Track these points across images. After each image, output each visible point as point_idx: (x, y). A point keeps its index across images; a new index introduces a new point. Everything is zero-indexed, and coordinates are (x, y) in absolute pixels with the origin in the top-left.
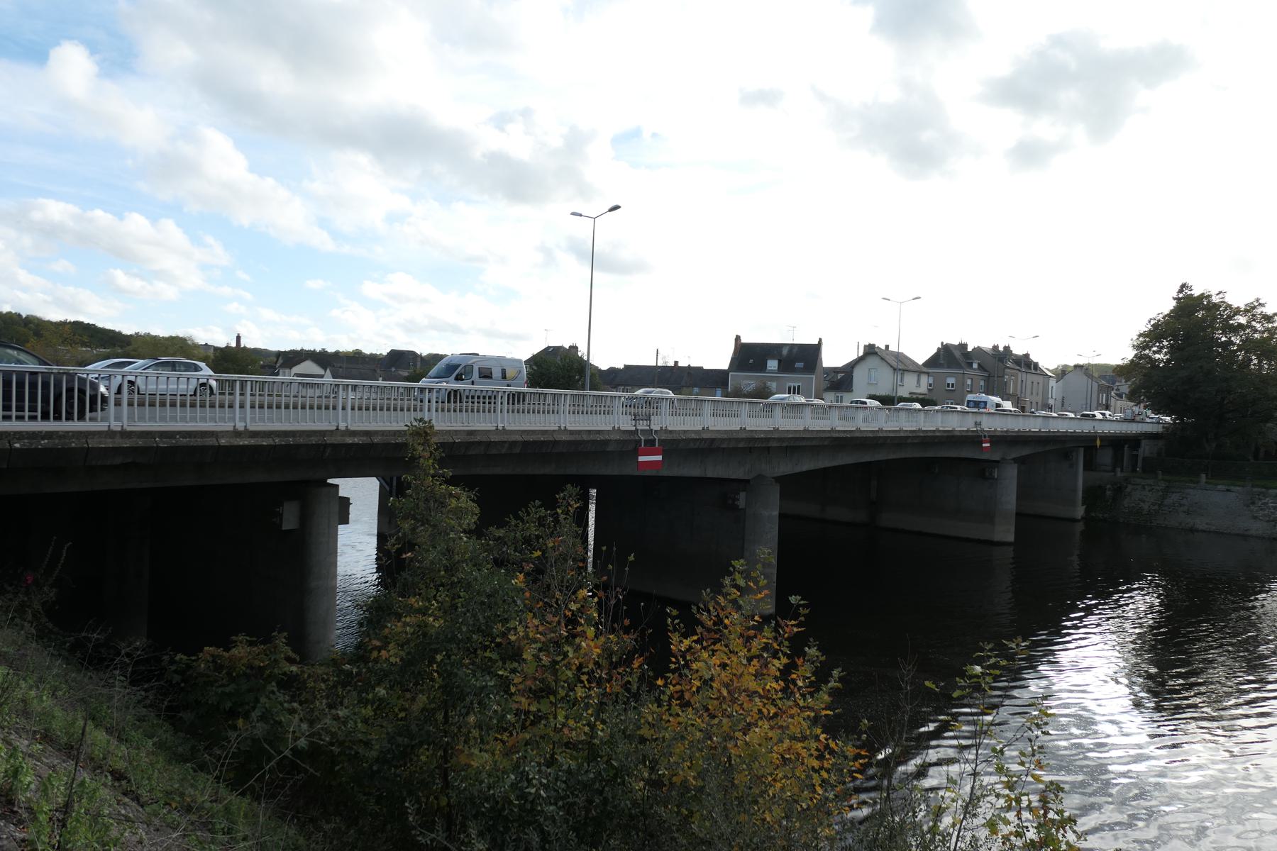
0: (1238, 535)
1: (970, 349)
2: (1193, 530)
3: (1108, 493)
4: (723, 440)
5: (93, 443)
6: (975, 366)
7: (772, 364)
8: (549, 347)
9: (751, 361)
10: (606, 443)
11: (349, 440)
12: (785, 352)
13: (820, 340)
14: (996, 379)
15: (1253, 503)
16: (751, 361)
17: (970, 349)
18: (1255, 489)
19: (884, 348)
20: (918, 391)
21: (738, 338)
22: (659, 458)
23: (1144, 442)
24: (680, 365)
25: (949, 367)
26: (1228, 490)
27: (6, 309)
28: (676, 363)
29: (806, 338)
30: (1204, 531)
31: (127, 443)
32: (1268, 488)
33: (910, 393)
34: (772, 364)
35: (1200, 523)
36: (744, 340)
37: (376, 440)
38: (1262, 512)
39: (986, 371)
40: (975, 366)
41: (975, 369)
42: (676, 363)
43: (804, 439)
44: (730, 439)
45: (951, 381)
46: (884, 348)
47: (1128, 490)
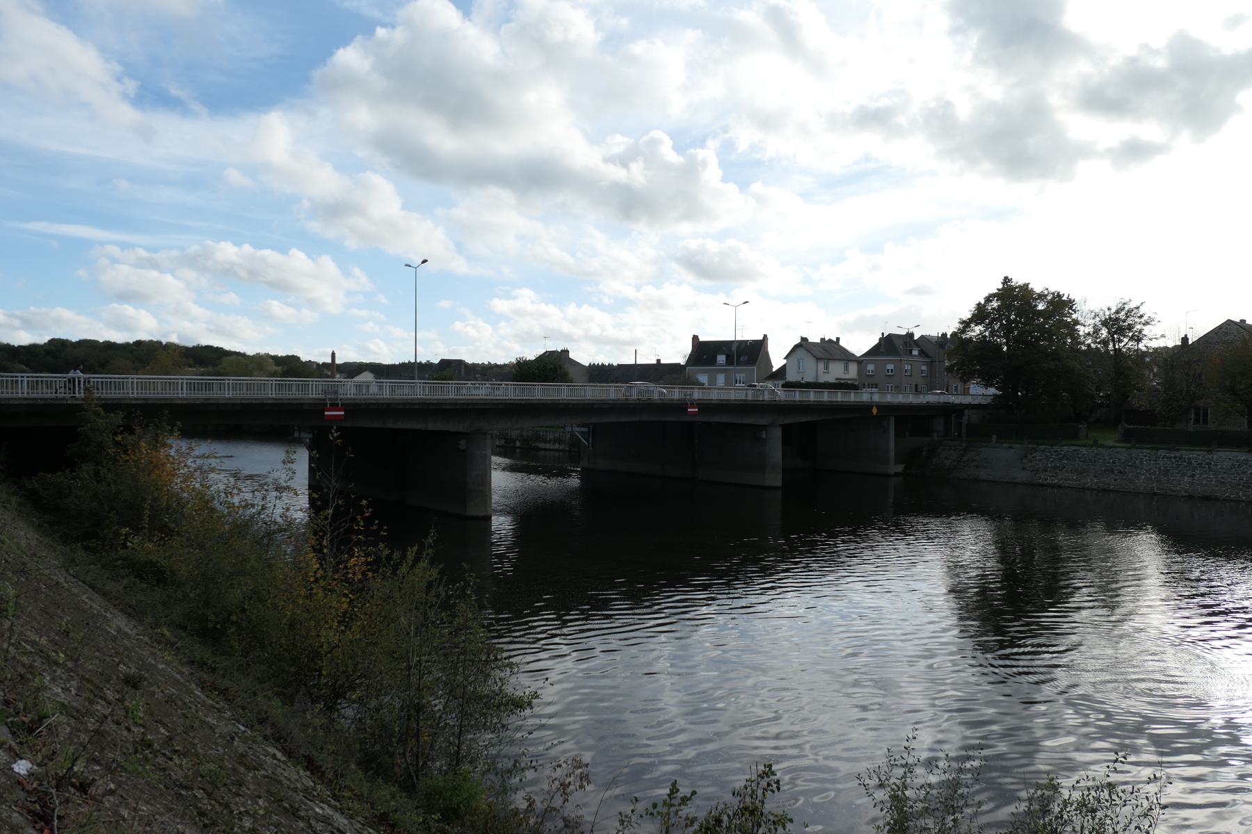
0: (1007, 482)
1: (916, 338)
2: (977, 480)
3: (924, 453)
4: (398, 404)
5: (11, 402)
6: (915, 352)
7: (721, 359)
8: (547, 352)
9: (705, 357)
10: (359, 405)
11: (134, 402)
12: (734, 348)
13: (765, 336)
14: (937, 363)
15: (1026, 457)
16: (705, 357)
17: (916, 338)
18: (1030, 446)
19: (835, 340)
20: (847, 376)
21: (695, 338)
22: (342, 413)
23: (966, 412)
24: (662, 362)
25: (888, 355)
26: (1010, 447)
27: (5, 341)
28: (658, 361)
29: (750, 334)
30: (984, 481)
31: (25, 402)
32: (1039, 445)
33: (837, 379)
34: (721, 359)
35: (983, 475)
36: (702, 339)
37: (149, 402)
38: (1029, 464)
39: (927, 356)
40: (915, 352)
41: (915, 356)
42: (658, 361)
43: (477, 404)
44: (404, 404)
45: (890, 367)
46: (835, 340)
47: (939, 450)
